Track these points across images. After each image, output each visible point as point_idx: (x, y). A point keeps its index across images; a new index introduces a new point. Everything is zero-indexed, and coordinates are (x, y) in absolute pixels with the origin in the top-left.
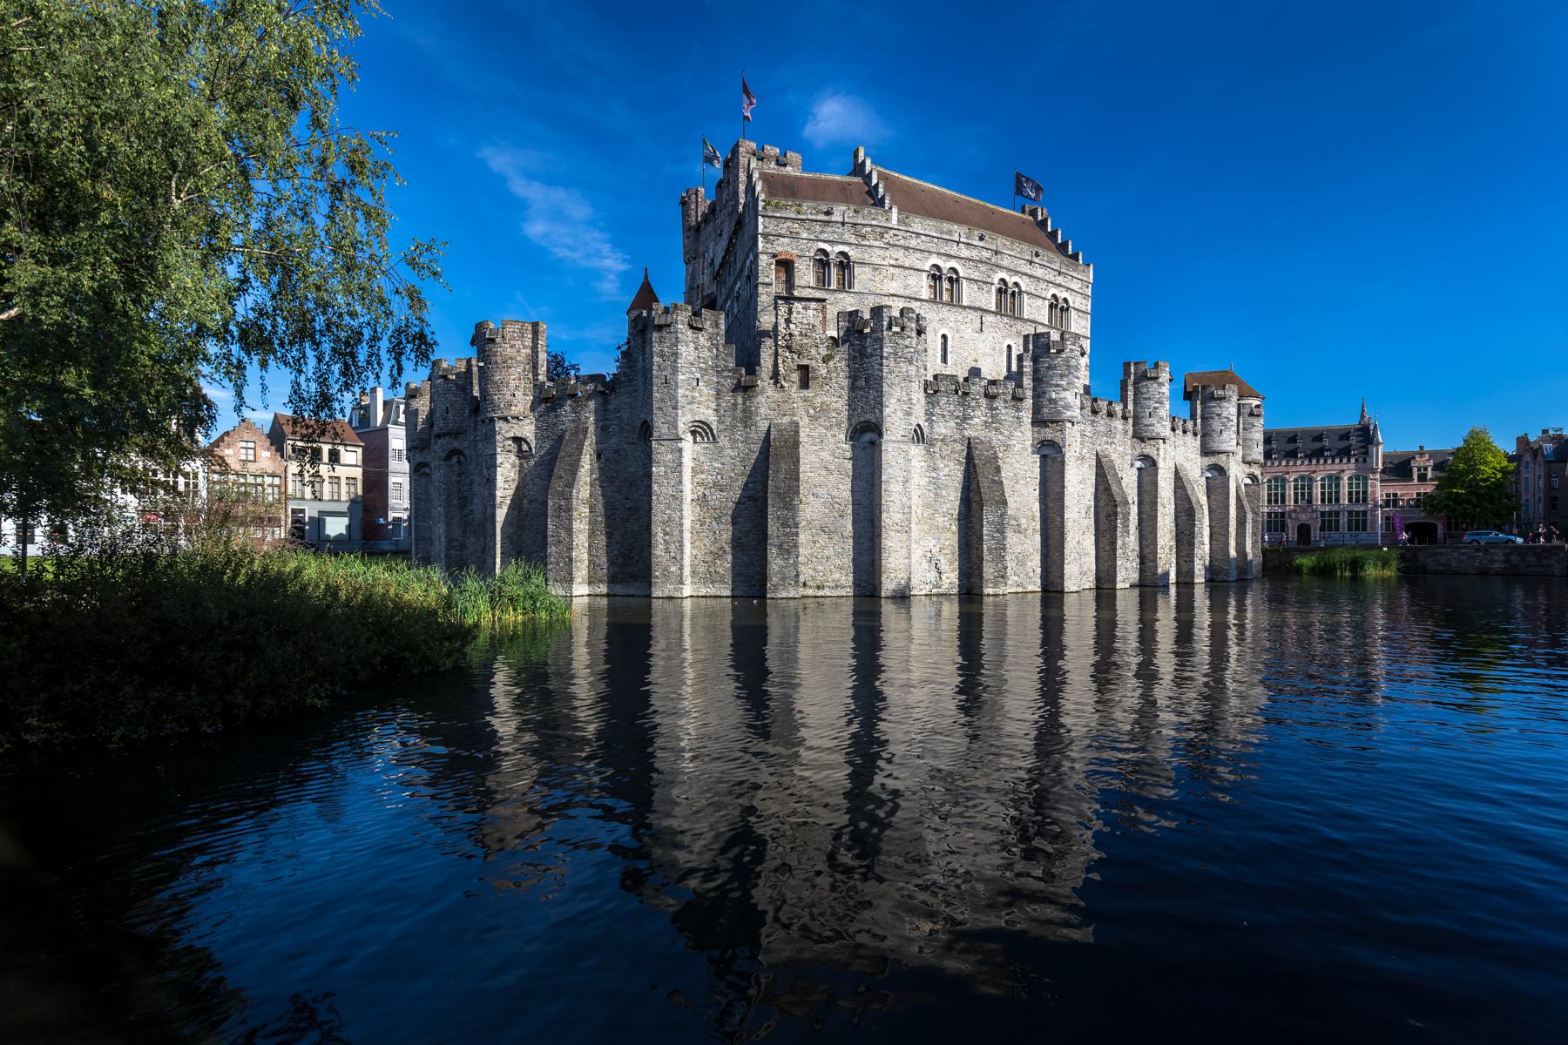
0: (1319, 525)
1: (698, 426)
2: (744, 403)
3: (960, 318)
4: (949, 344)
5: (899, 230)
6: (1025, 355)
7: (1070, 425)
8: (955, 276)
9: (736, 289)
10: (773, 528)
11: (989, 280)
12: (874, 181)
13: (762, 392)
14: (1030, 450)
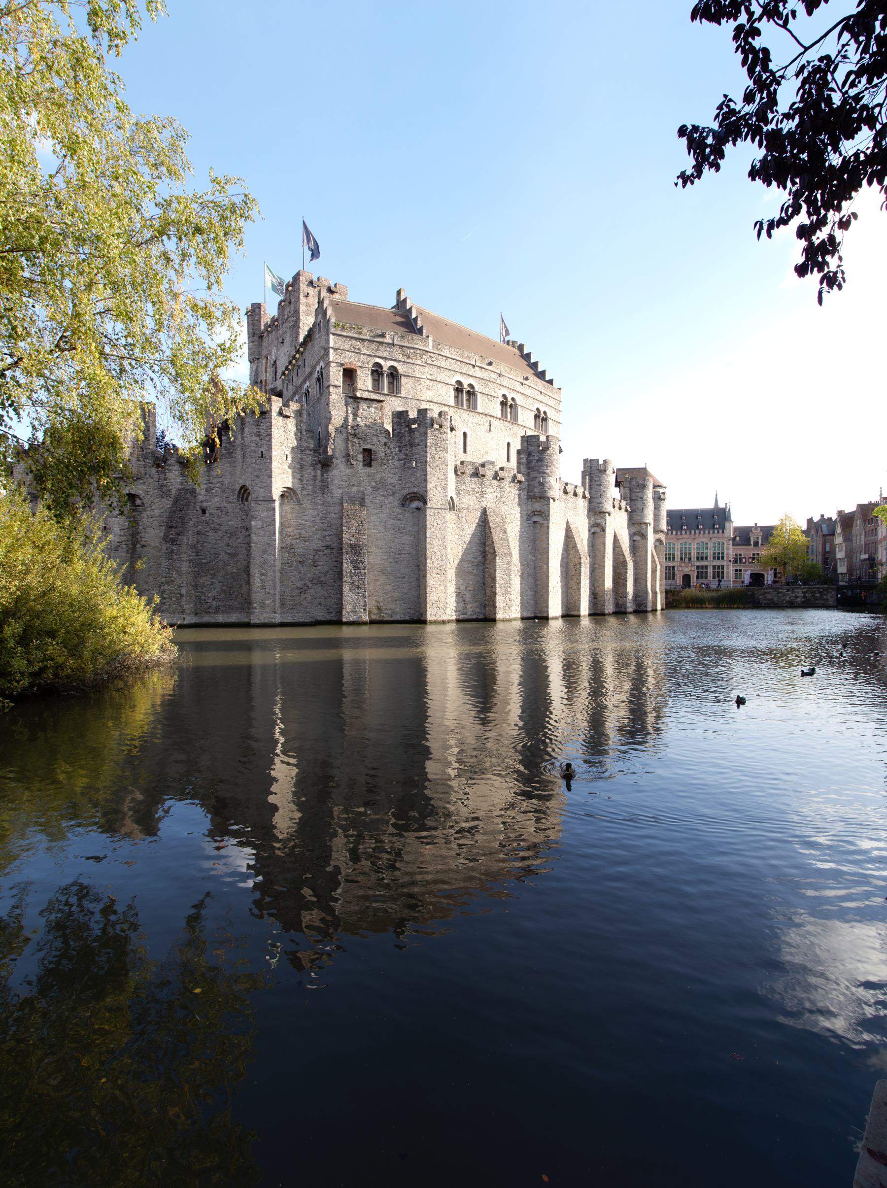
0: (696, 574)
2: (322, 475)
3: (476, 421)
7: (551, 501)
9: (305, 386)
10: (347, 567)
11: (495, 395)
12: (414, 316)
13: (336, 468)
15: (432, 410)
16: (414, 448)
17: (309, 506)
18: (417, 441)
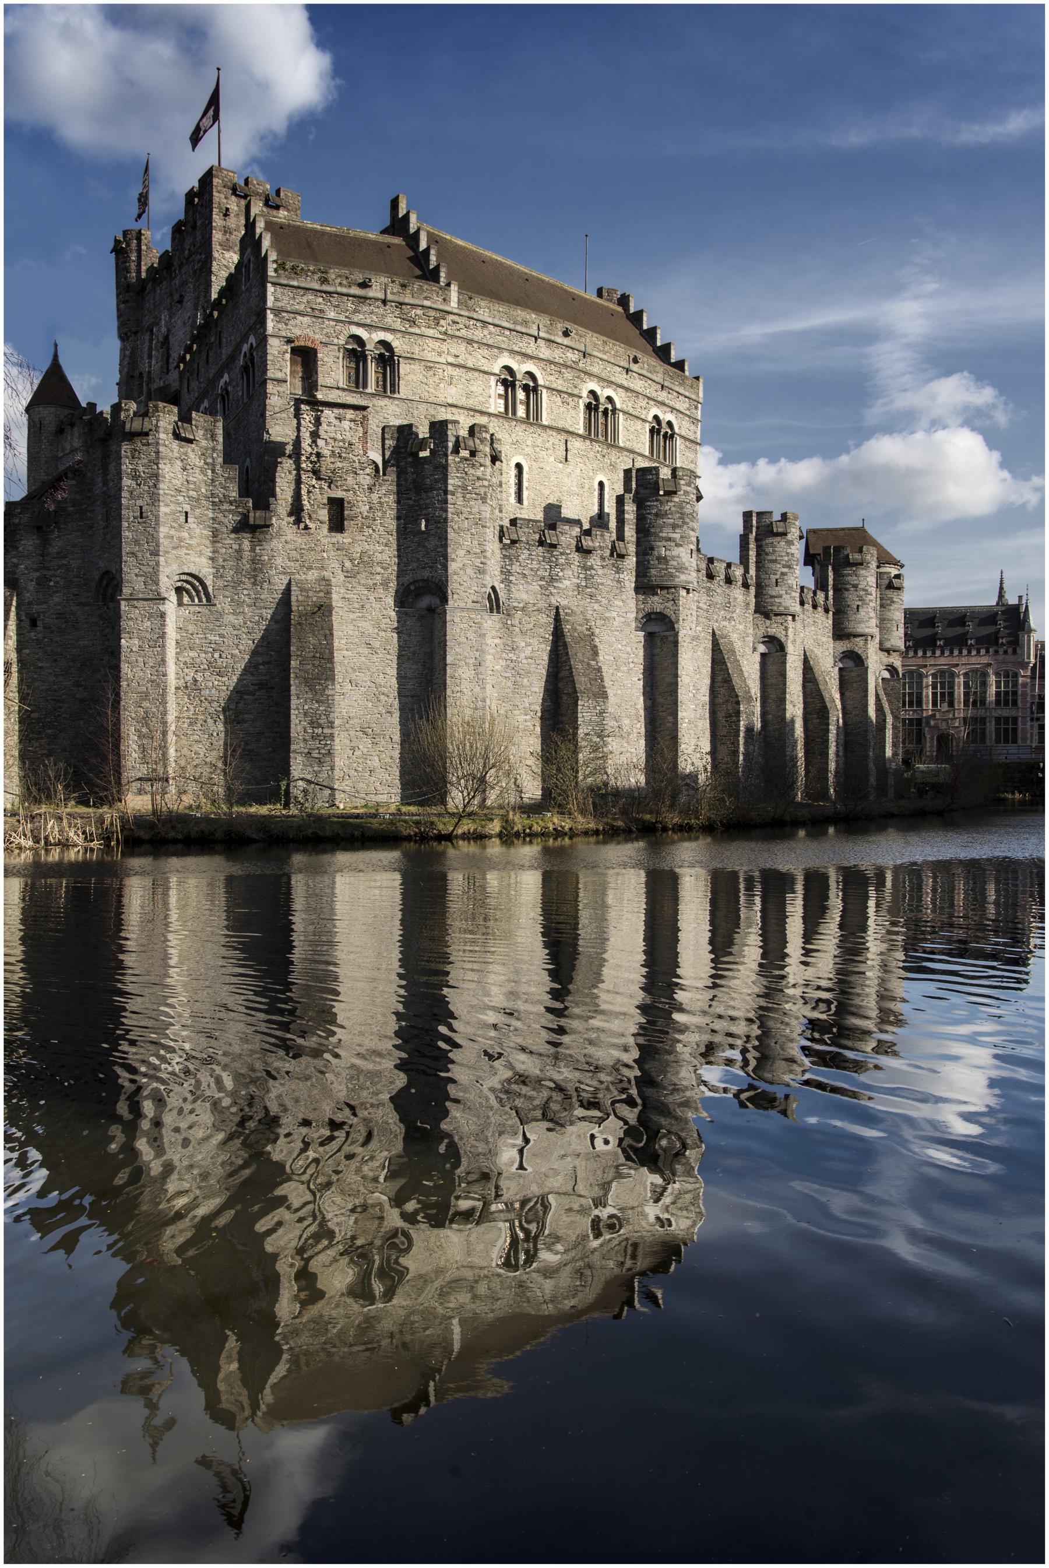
1: (187, 582)
2: (253, 550)
3: (539, 441)
4: (525, 476)
5: (460, 315)
6: (627, 496)
7: (683, 593)
8: (531, 384)
11: (576, 392)
12: (423, 245)
13: (279, 535)
14: (634, 625)
15: (456, 422)
16: (424, 495)
17: (228, 609)
18: (428, 481)
